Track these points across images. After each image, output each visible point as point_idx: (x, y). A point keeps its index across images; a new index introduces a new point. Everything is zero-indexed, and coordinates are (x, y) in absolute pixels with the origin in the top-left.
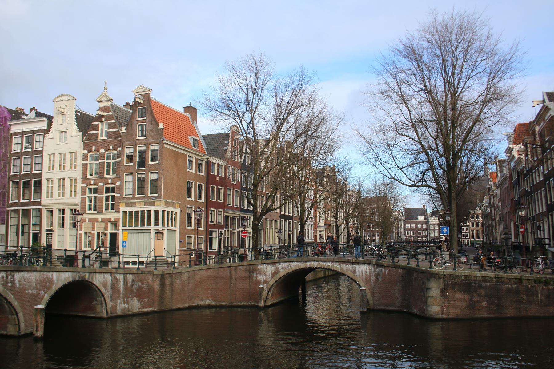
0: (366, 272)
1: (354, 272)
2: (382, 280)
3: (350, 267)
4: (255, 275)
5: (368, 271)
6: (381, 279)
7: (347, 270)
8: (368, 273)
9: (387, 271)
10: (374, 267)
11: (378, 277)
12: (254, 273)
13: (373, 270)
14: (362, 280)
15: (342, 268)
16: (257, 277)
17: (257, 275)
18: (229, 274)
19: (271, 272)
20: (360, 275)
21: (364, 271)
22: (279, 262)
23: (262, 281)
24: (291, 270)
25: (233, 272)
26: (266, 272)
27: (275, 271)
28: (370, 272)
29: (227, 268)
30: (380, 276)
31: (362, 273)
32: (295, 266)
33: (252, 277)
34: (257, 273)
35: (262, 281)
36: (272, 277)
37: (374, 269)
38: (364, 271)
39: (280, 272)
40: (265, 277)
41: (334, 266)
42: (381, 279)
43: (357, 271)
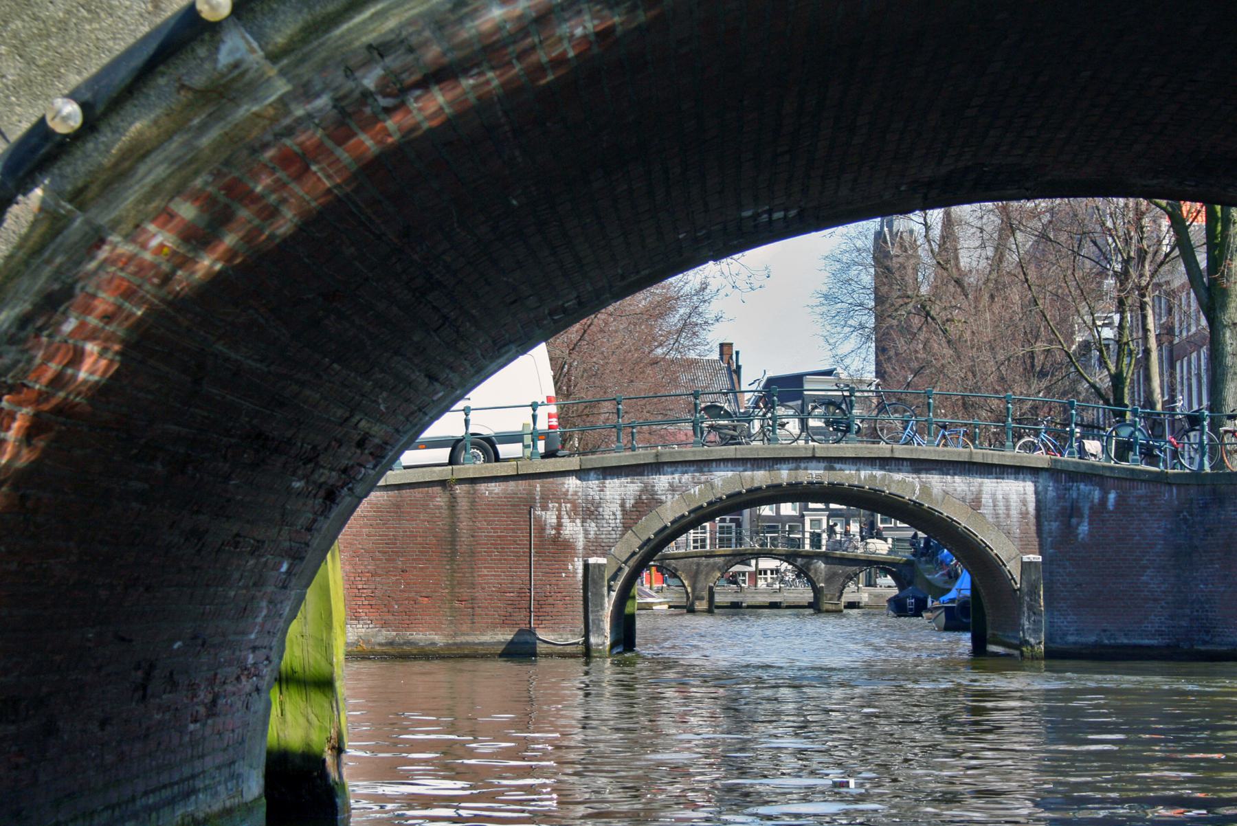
0: (1024, 502)
1: (976, 503)
2: (1091, 534)
3: (959, 484)
4: (550, 517)
5: (1031, 498)
6: (1084, 528)
7: (947, 493)
8: (1031, 507)
9: (1112, 496)
10: (1057, 481)
11: (1074, 521)
12: (545, 508)
13: (1051, 493)
14: (1008, 534)
15: (925, 489)
16: (559, 526)
17: (559, 517)
18: (445, 512)
19: (623, 505)
20: (997, 516)
21: (1014, 498)
22: (657, 467)
23: (580, 544)
24: (712, 498)
25: (463, 504)
26: (599, 505)
27: (639, 502)
28: (1038, 501)
29: (438, 489)
30: (1081, 516)
31: (1008, 508)
32: (726, 481)
33: (542, 528)
34: (559, 510)
35: (580, 544)
36: (626, 527)
37: (1057, 489)
38: (1014, 498)
39: (661, 502)
40: (592, 527)
41: (892, 481)
42: (1084, 528)
43: (986, 499)
